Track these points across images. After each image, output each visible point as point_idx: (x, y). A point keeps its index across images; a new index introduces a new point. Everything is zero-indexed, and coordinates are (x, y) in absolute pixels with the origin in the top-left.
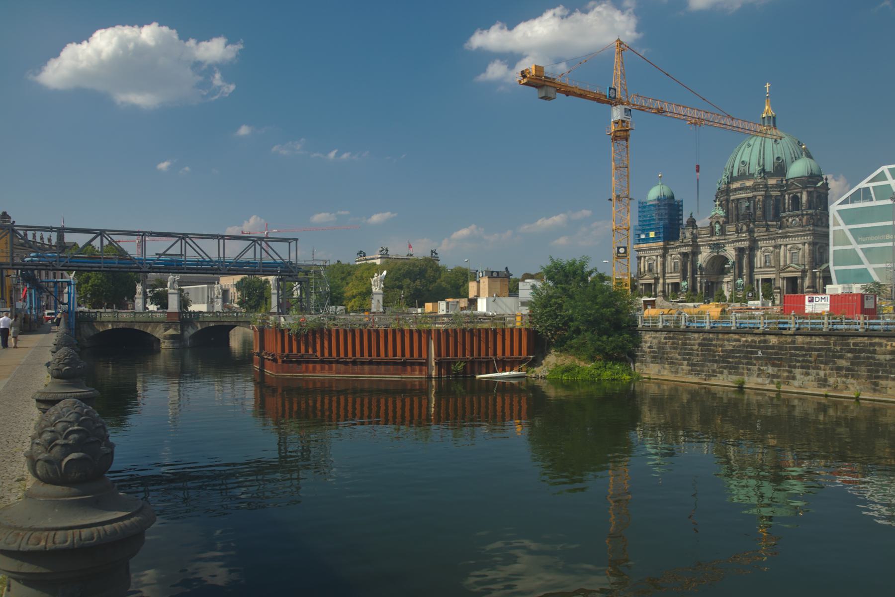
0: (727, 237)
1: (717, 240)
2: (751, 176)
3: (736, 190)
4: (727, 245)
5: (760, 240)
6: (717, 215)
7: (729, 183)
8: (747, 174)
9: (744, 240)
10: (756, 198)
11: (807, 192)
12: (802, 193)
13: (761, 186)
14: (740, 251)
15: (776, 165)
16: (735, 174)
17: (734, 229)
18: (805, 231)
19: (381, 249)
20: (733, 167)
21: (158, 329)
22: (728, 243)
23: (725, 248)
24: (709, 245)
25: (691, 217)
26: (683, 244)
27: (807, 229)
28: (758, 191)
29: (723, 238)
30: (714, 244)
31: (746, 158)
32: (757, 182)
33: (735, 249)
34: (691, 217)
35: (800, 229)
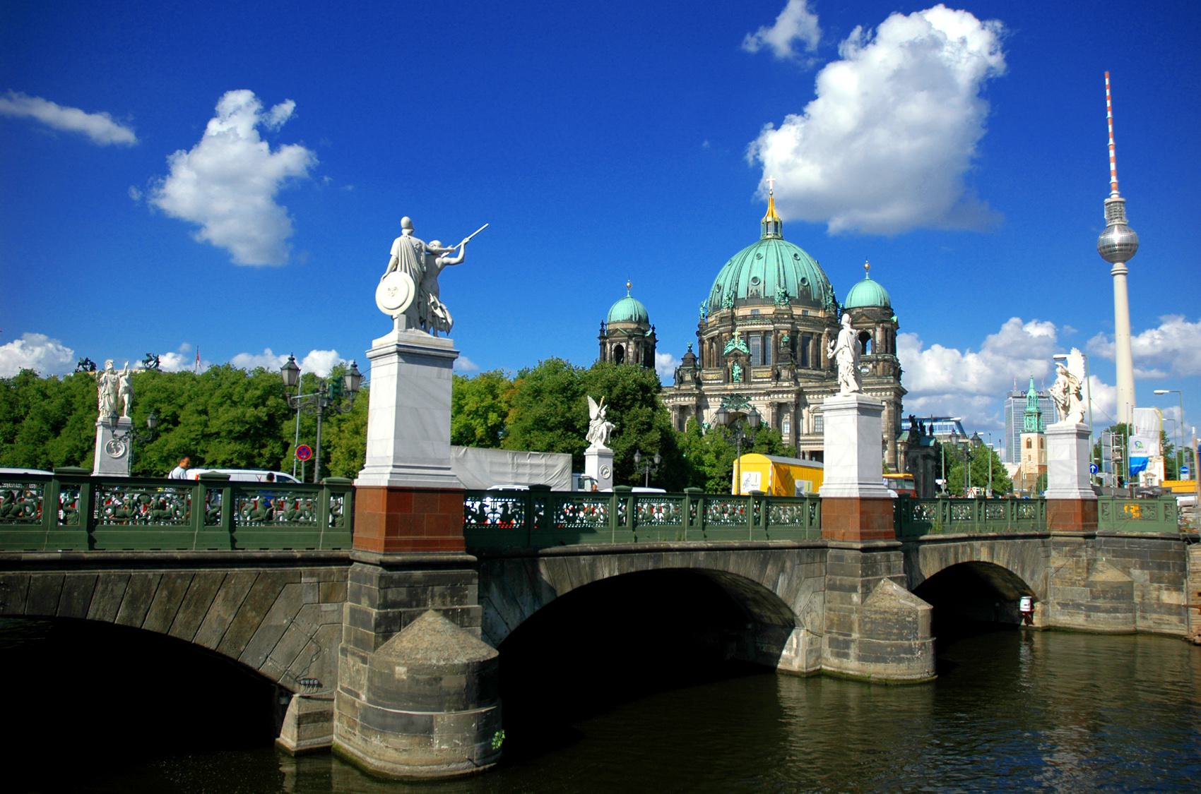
0: (753, 386)
1: (735, 389)
2: (769, 301)
3: (745, 318)
4: (753, 398)
5: (809, 393)
6: (736, 351)
7: (734, 307)
9: (788, 392)
10: (778, 332)
11: (883, 328)
12: (875, 330)
13: (786, 316)
14: (780, 408)
15: (801, 289)
16: (742, 294)
17: (769, 374)
18: (883, 384)
19: (147, 358)
20: (737, 284)
21: (279, 616)
22: (756, 395)
23: (749, 402)
24: (723, 396)
25: (690, 351)
26: (678, 392)
27: (885, 381)
28: (782, 323)
29: (747, 386)
30: (732, 396)
31: (757, 272)
32: (780, 310)
33: (771, 404)
34: (690, 351)
35: (876, 380)
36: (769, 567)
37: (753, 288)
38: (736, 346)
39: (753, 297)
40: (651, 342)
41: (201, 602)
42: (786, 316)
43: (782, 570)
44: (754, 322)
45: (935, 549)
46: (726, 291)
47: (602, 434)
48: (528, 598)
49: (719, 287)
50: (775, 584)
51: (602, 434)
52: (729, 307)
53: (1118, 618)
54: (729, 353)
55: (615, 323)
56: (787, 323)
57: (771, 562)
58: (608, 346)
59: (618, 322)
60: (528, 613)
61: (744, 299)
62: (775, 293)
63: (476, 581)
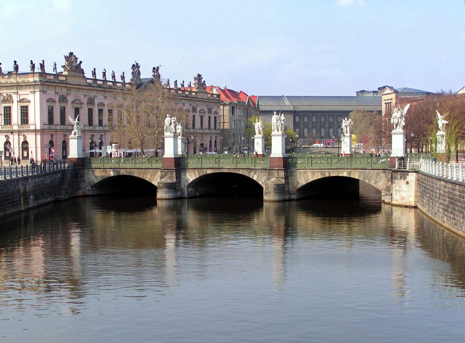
36: (251, 173)
41: (147, 174)
43: (256, 173)
45: (319, 171)
48: (194, 176)
50: (253, 177)
53: (387, 198)
57: (252, 172)
60: (194, 179)
63: (175, 172)
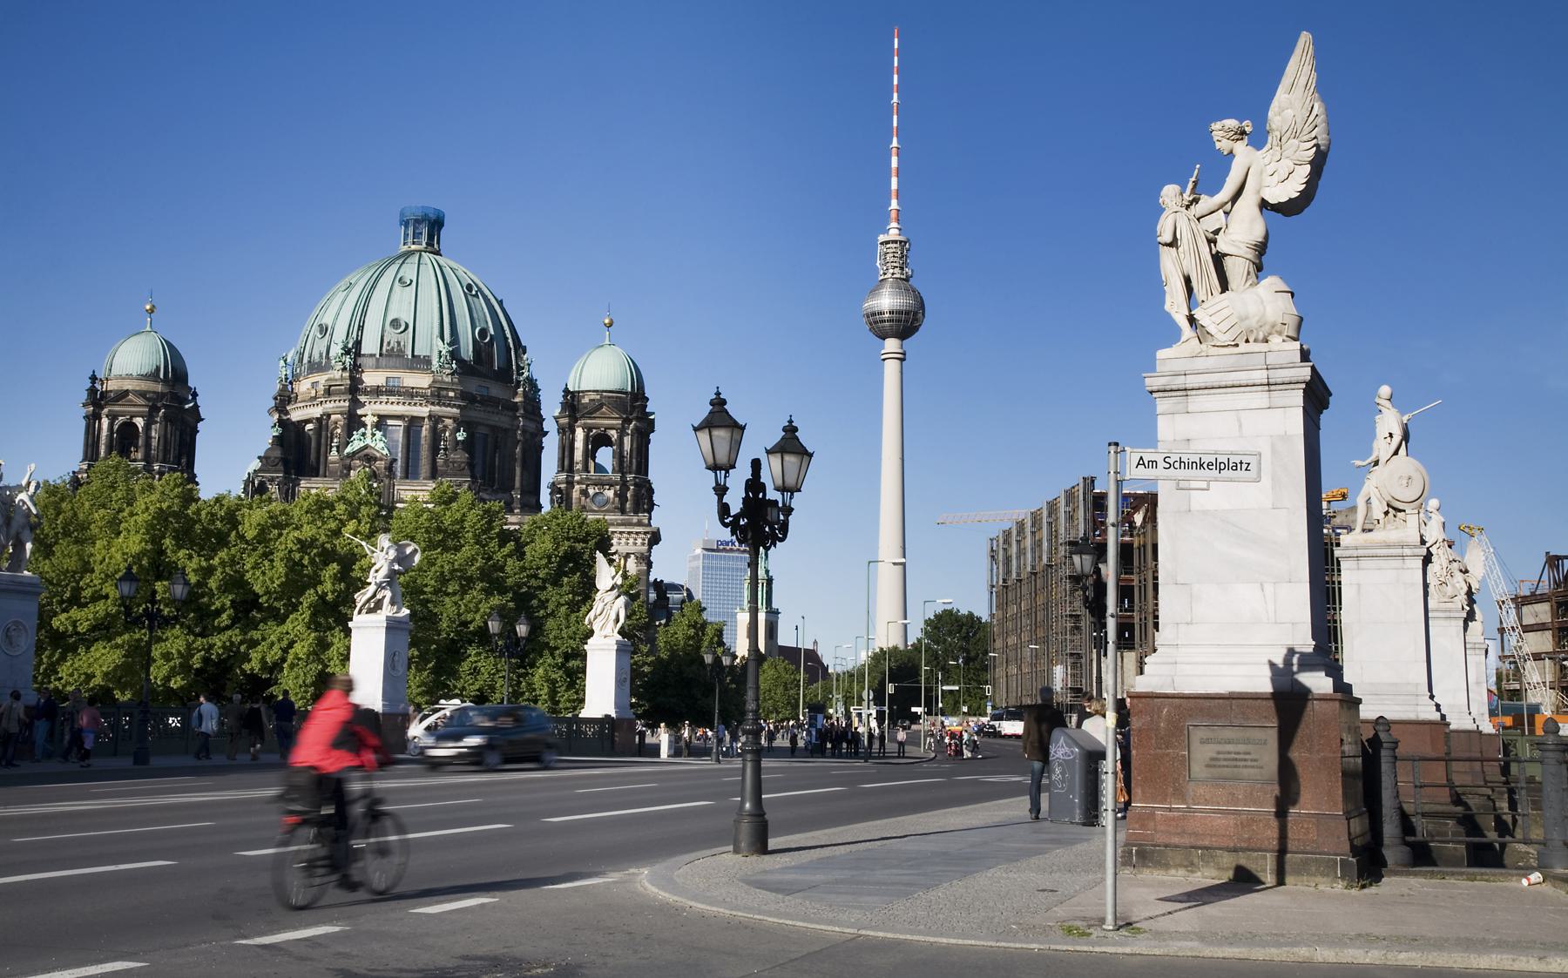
2: (419, 363)
8: (410, 357)
16: (370, 346)
18: (630, 524)
20: (361, 328)
27: (635, 519)
28: (444, 405)
37: (392, 336)
38: (368, 441)
39: (390, 353)
40: (190, 420)
42: (451, 394)
44: (392, 399)
46: (339, 336)
47: (618, 615)
49: (324, 330)
51: (618, 615)
52: (344, 369)
54: (354, 453)
55: (120, 377)
56: (454, 406)
58: (105, 422)
59: (129, 377)
61: (372, 355)
62: (431, 350)
